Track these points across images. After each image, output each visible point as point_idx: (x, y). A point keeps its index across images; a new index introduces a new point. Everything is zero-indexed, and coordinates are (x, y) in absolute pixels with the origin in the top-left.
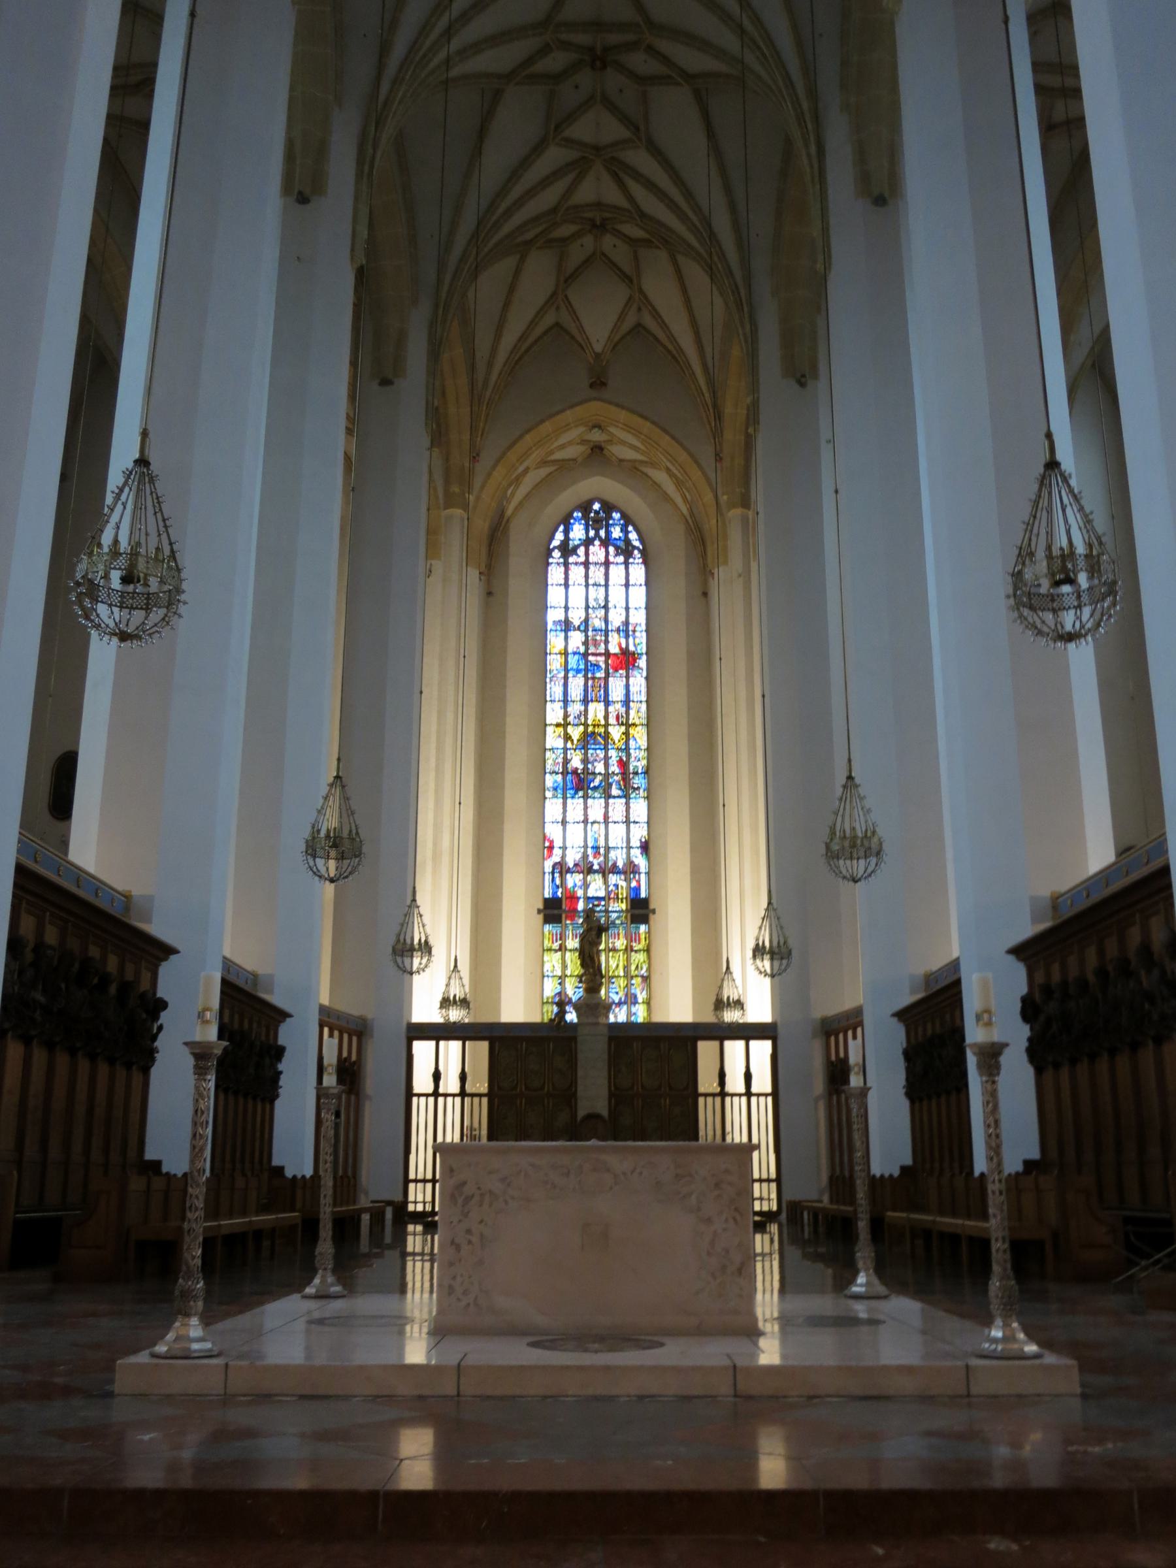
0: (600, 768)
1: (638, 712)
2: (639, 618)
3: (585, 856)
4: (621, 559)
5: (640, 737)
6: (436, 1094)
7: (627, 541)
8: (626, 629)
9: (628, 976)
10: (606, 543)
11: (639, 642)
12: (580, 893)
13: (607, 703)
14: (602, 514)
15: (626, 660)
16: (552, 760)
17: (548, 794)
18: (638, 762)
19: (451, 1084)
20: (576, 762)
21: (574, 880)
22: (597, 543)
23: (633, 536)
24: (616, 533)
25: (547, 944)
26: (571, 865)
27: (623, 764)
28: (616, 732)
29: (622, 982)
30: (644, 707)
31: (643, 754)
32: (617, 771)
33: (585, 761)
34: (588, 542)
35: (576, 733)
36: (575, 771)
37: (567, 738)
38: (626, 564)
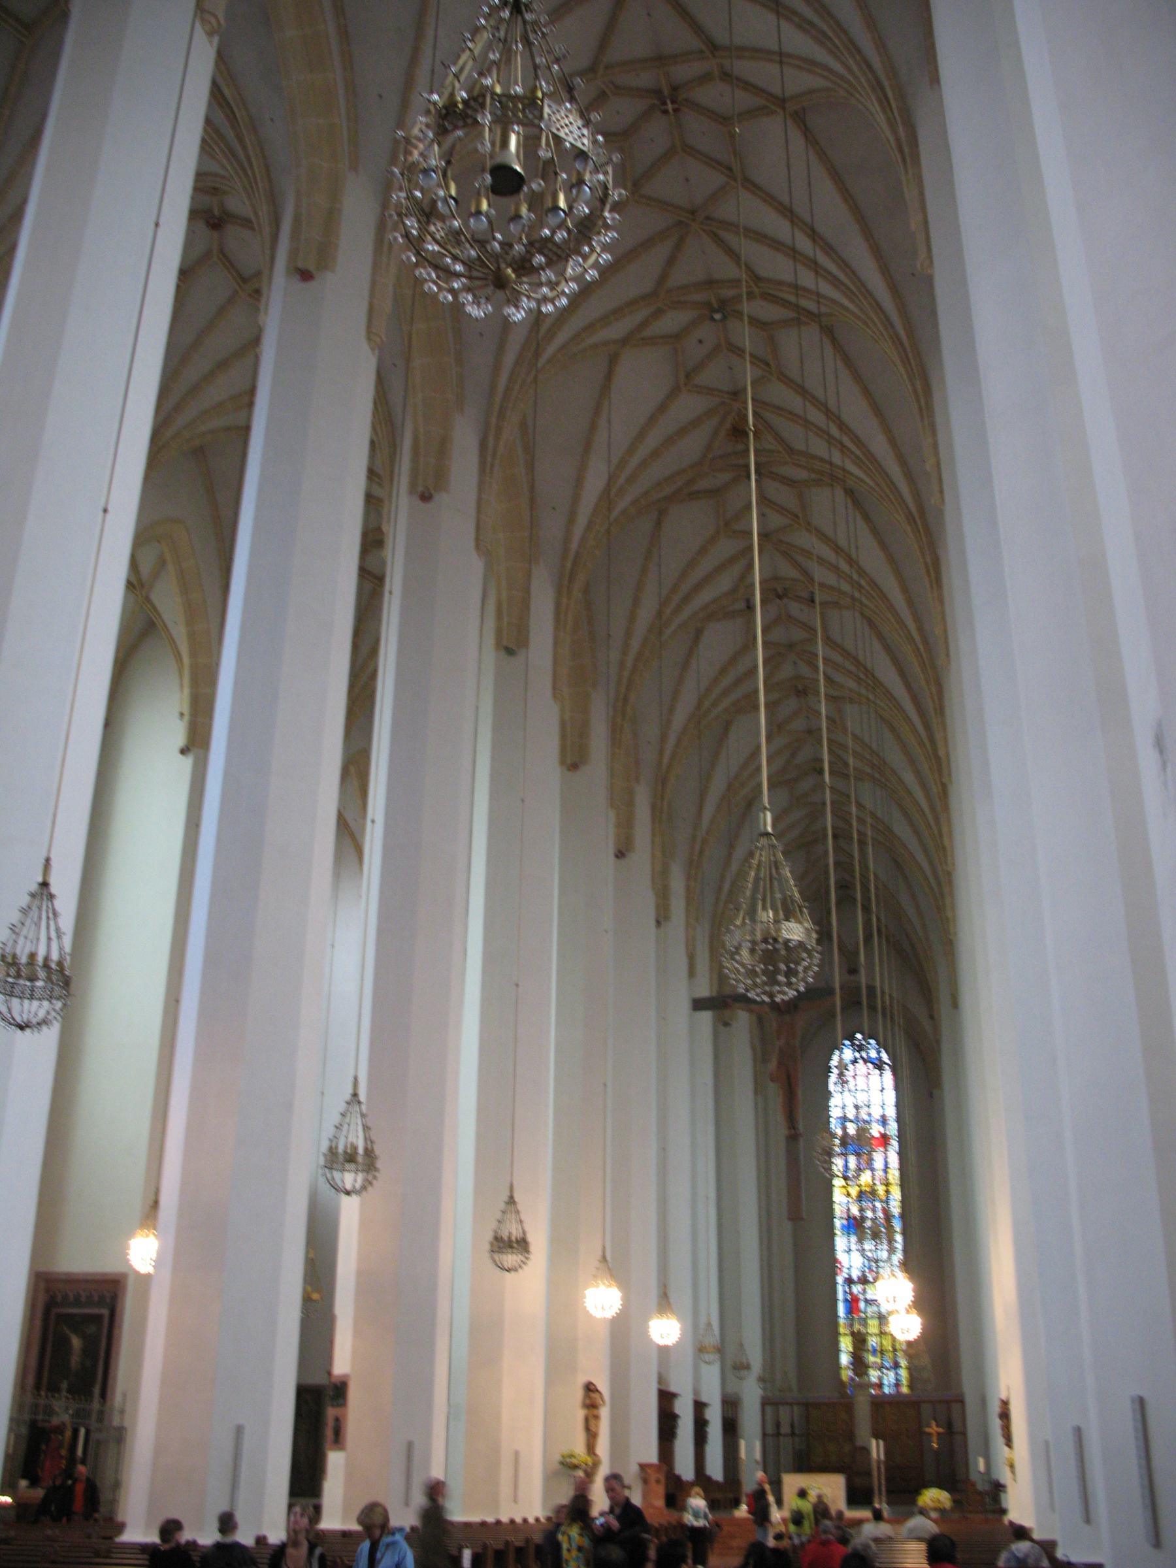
0: (869, 1214)
1: (894, 1175)
2: (891, 1112)
3: (863, 1272)
4: (877, 1072)
5: (896, 1193)
6: (778, 1434)
7: (880, 1059)
8: (884, 1121)
9: (895, 1350)
10: (865, 1061)
11: (893, 1128)
12: (861, 1297)
13: (873, 1170)
14: (864, 1043)
15: (884, 1140)
16: (838, 1210)
17: (837, 1232)
18: (895, 1208)
19: (785, 1429)
20: (855, 1211)
21: (857, 1289)
22: (861, 1061)
23: (885, 1057)
24: (873, 1054)
25: (842, 1330)
26: (855, 1278)
27: (886, 1212)
28: (881, 1190)
29: (891, 1355)
30: (897, 1173)
31: (898, 1204)
32: (881, 1215)
33: (861, 1210)
34: (855, 1061)
35: (854, 1191)
36: (855, 1218)
37: (848, 1195)
38: (881, 1075)
